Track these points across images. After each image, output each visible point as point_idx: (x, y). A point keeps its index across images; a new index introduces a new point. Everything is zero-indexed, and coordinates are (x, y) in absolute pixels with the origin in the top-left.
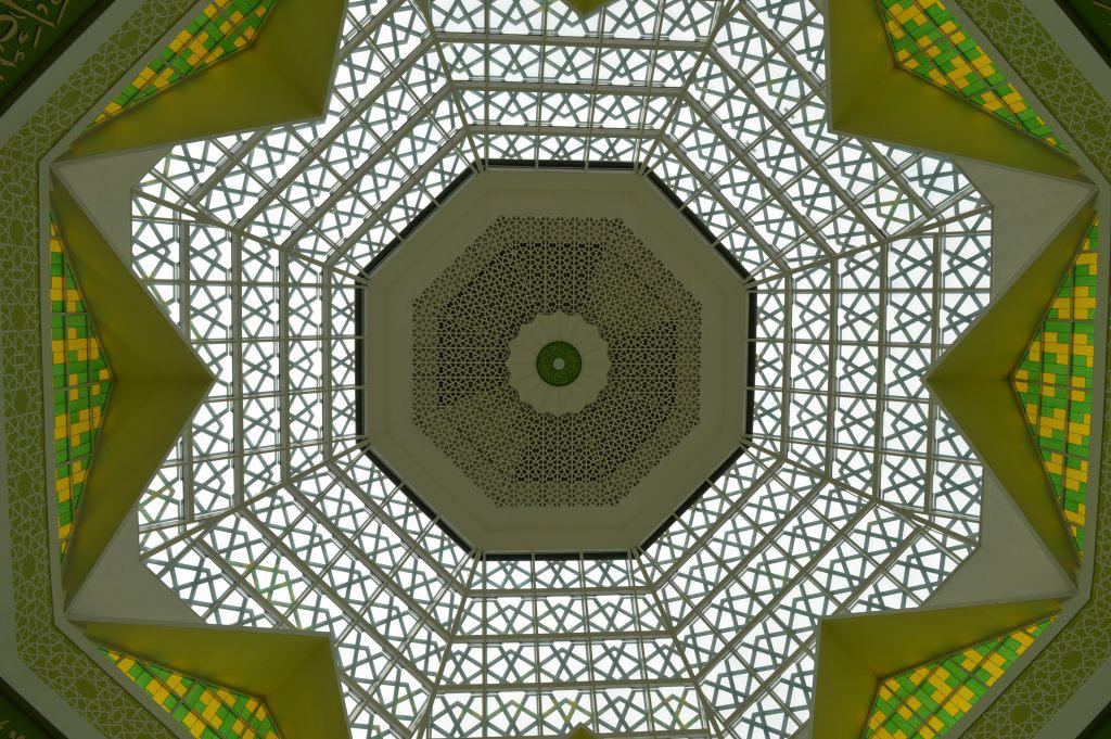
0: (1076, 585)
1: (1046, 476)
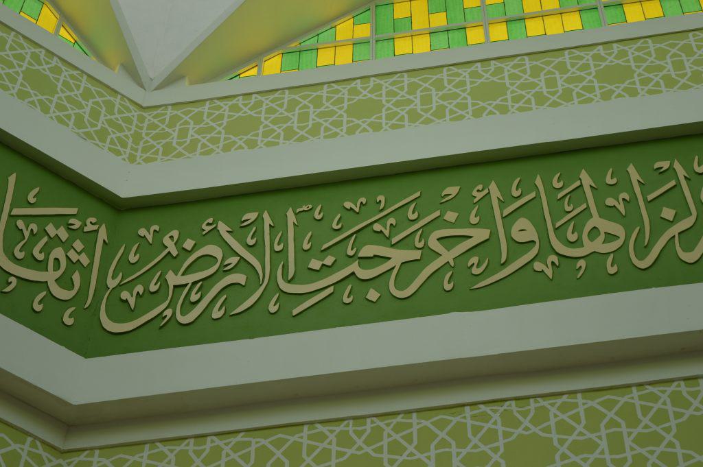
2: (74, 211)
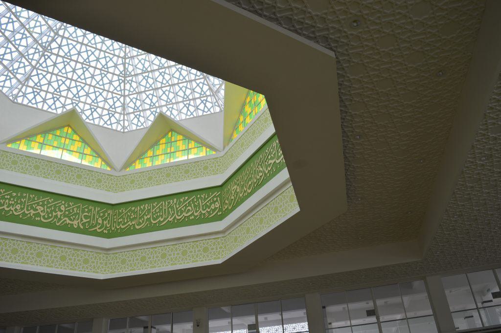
0: (120, 171)
1: (146, 151)
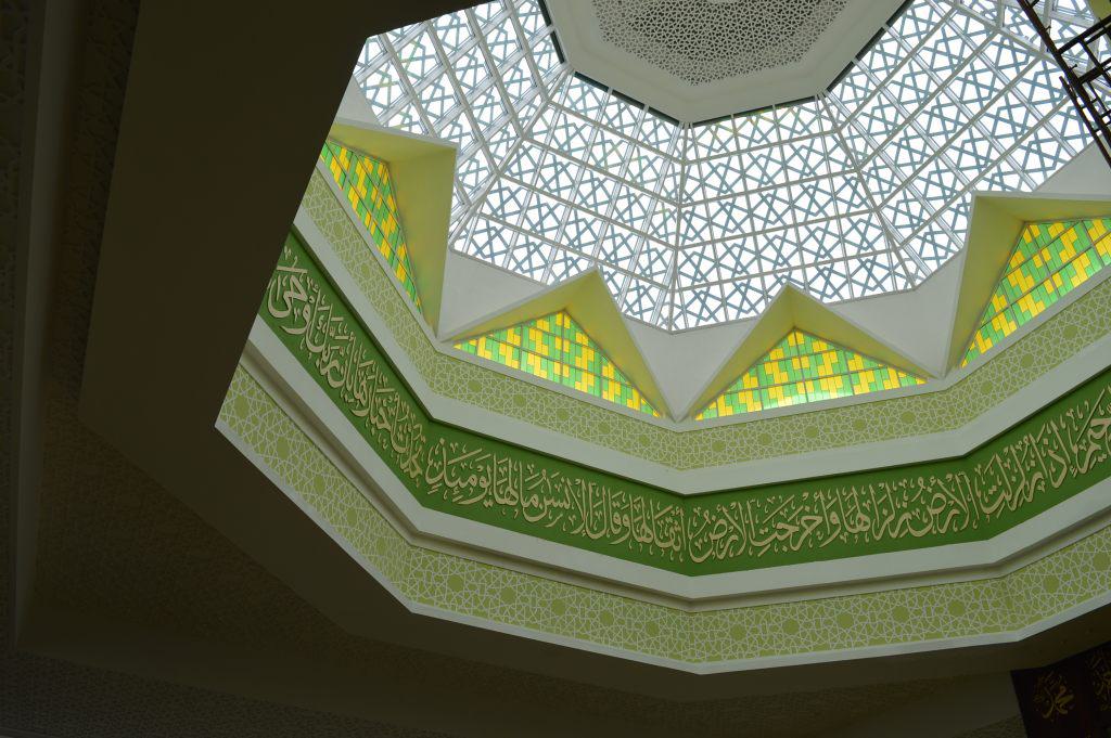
1: (988, 302)
2: (671, 507)
